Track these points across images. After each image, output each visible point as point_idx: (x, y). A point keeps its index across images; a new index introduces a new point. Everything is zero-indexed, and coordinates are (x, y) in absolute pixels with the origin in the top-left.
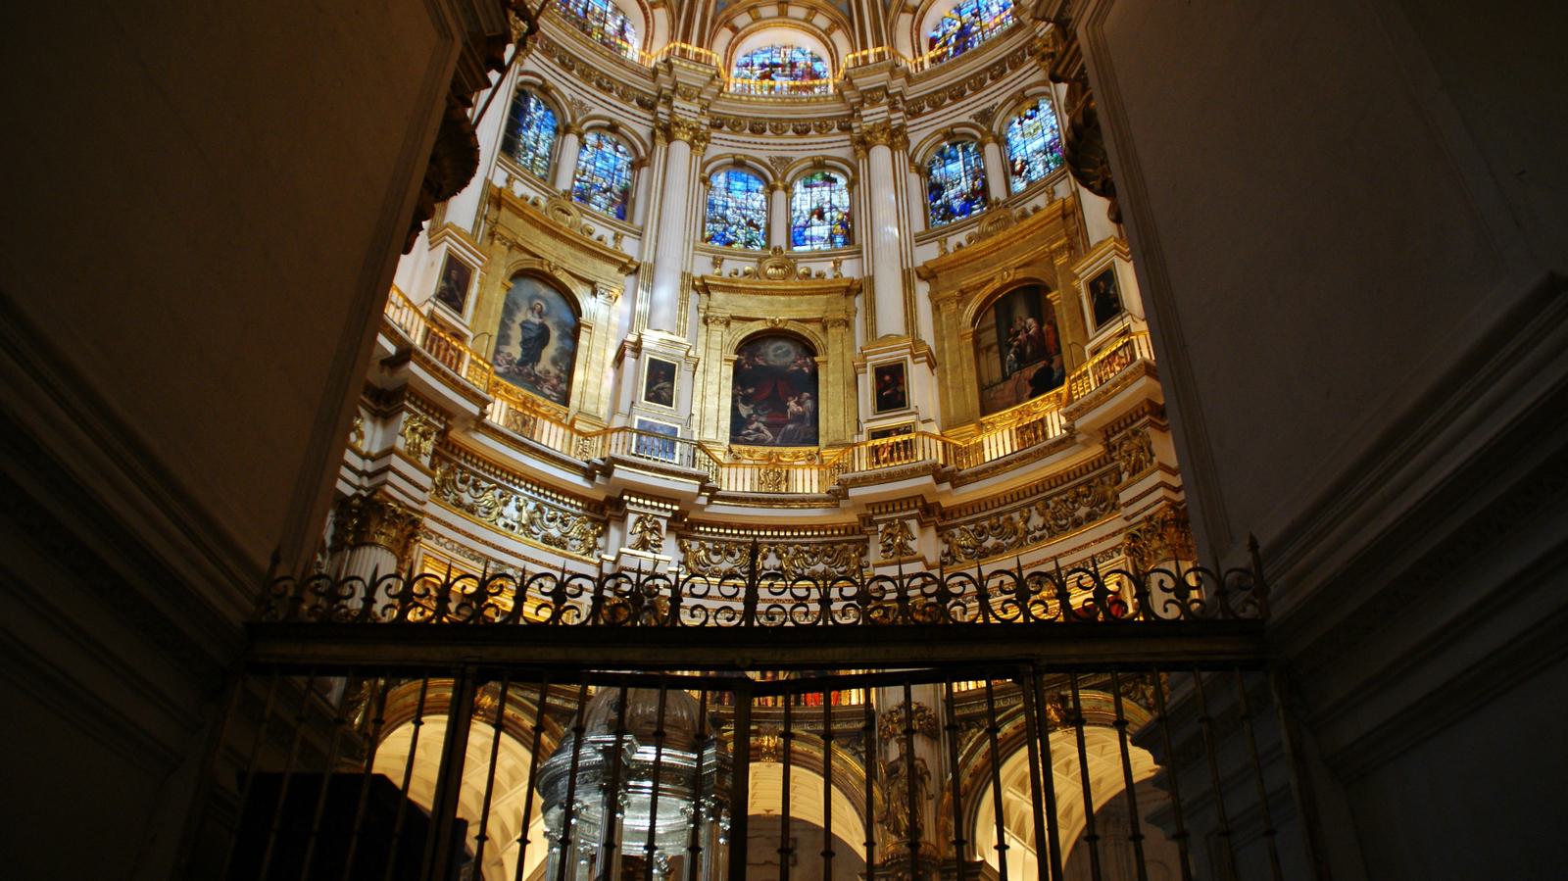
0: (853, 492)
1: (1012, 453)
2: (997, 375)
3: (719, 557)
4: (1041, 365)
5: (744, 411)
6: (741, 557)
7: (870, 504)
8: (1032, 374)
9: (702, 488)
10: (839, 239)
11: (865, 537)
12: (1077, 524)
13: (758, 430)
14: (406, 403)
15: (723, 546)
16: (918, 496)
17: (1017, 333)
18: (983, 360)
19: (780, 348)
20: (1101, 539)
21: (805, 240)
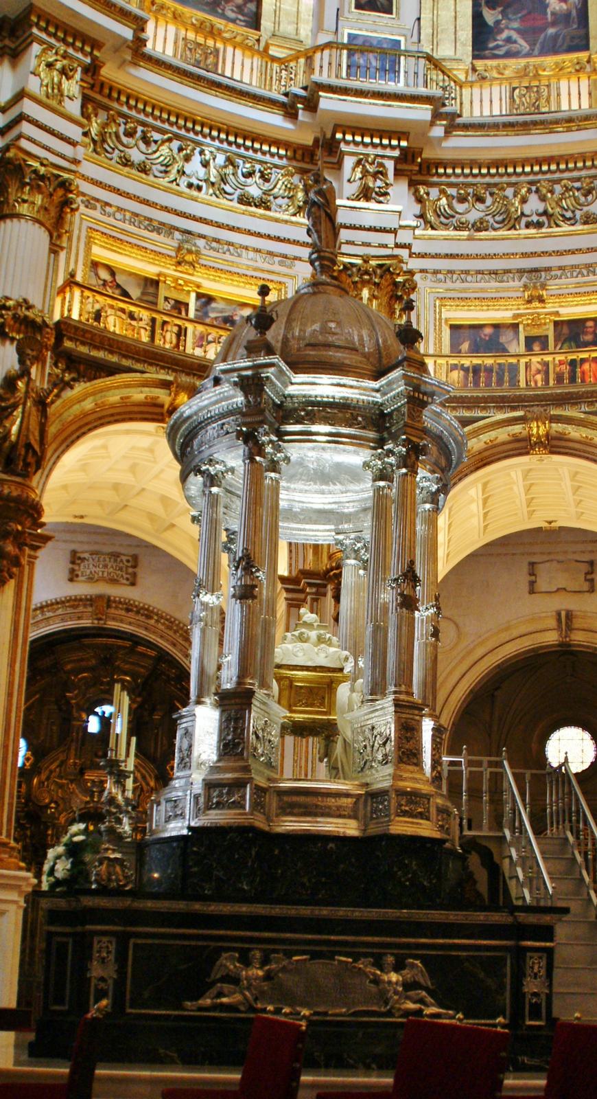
3: (466, 205)
5: (490, 16)
6: (493, 203)
9: (437, 116)
13: (509, 40)
14: (35, 30)
15: (470, 190)
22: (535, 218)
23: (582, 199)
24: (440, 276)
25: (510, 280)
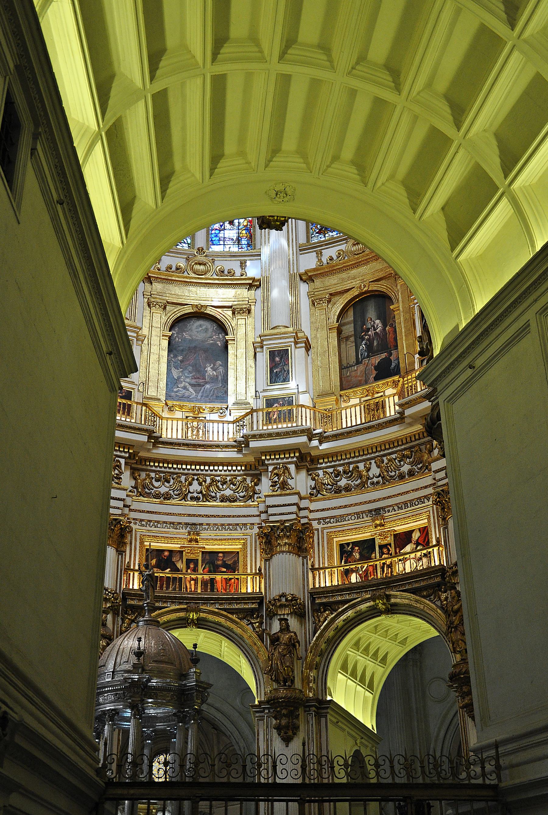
0: (252, 444)
1: (361, 424)
2: (353, 360)
4: (383, 356)
6: (174, 483)
7: (263, 452)
8: (377, 362)
9: (150, 437)
10: (244, 242)
11: (259, 472)
12: (402, 477)
13: (185, 388)
15: (162, 475)
16: (297, 449)
17: (368, 330)
18: (343, 346)
19: (201, 326)
20: (417, 490)
21: (219, 240)
22: (195, 495)
23: (221, 487)
24: (143, 523)
25: (180, 528)
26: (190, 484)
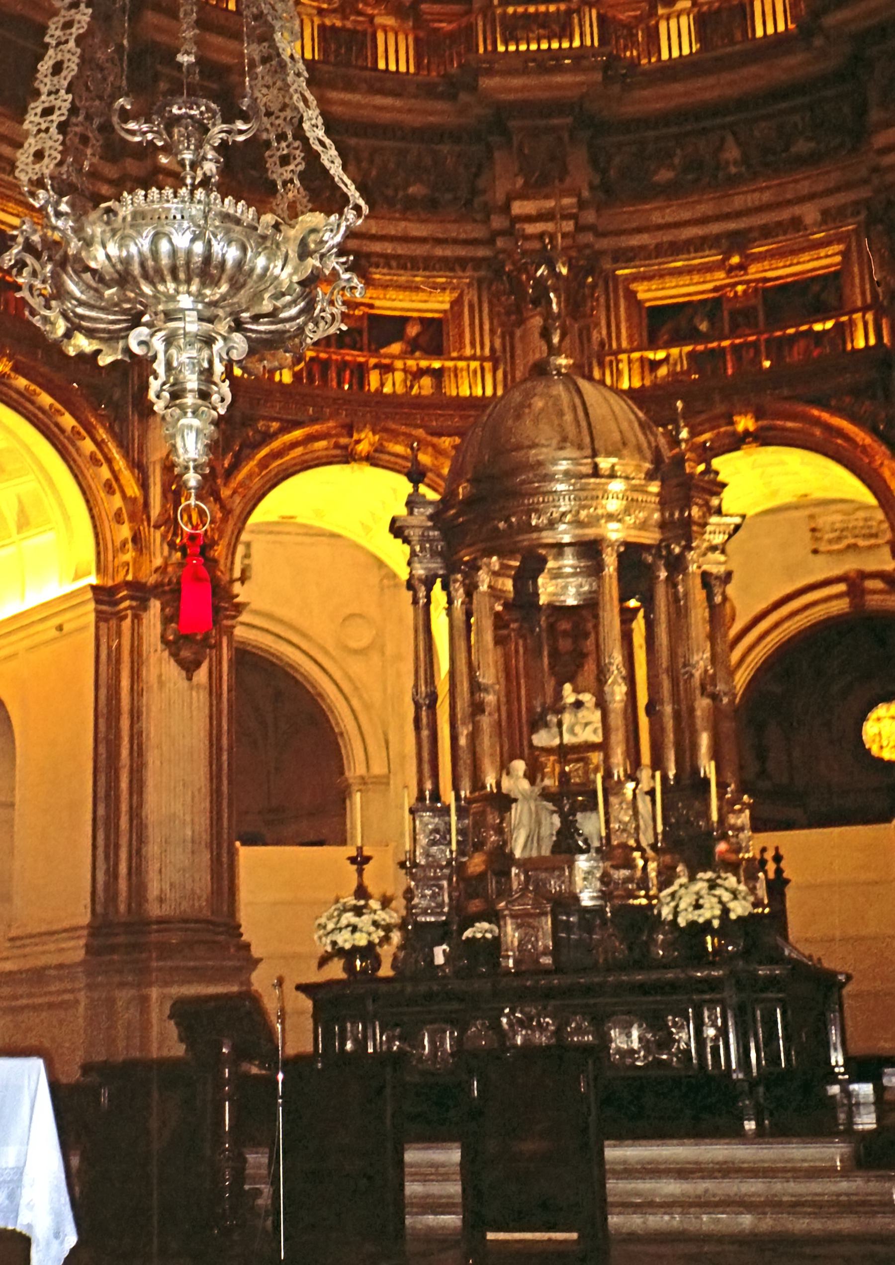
22: (733, 170)
26: (720, 148)
